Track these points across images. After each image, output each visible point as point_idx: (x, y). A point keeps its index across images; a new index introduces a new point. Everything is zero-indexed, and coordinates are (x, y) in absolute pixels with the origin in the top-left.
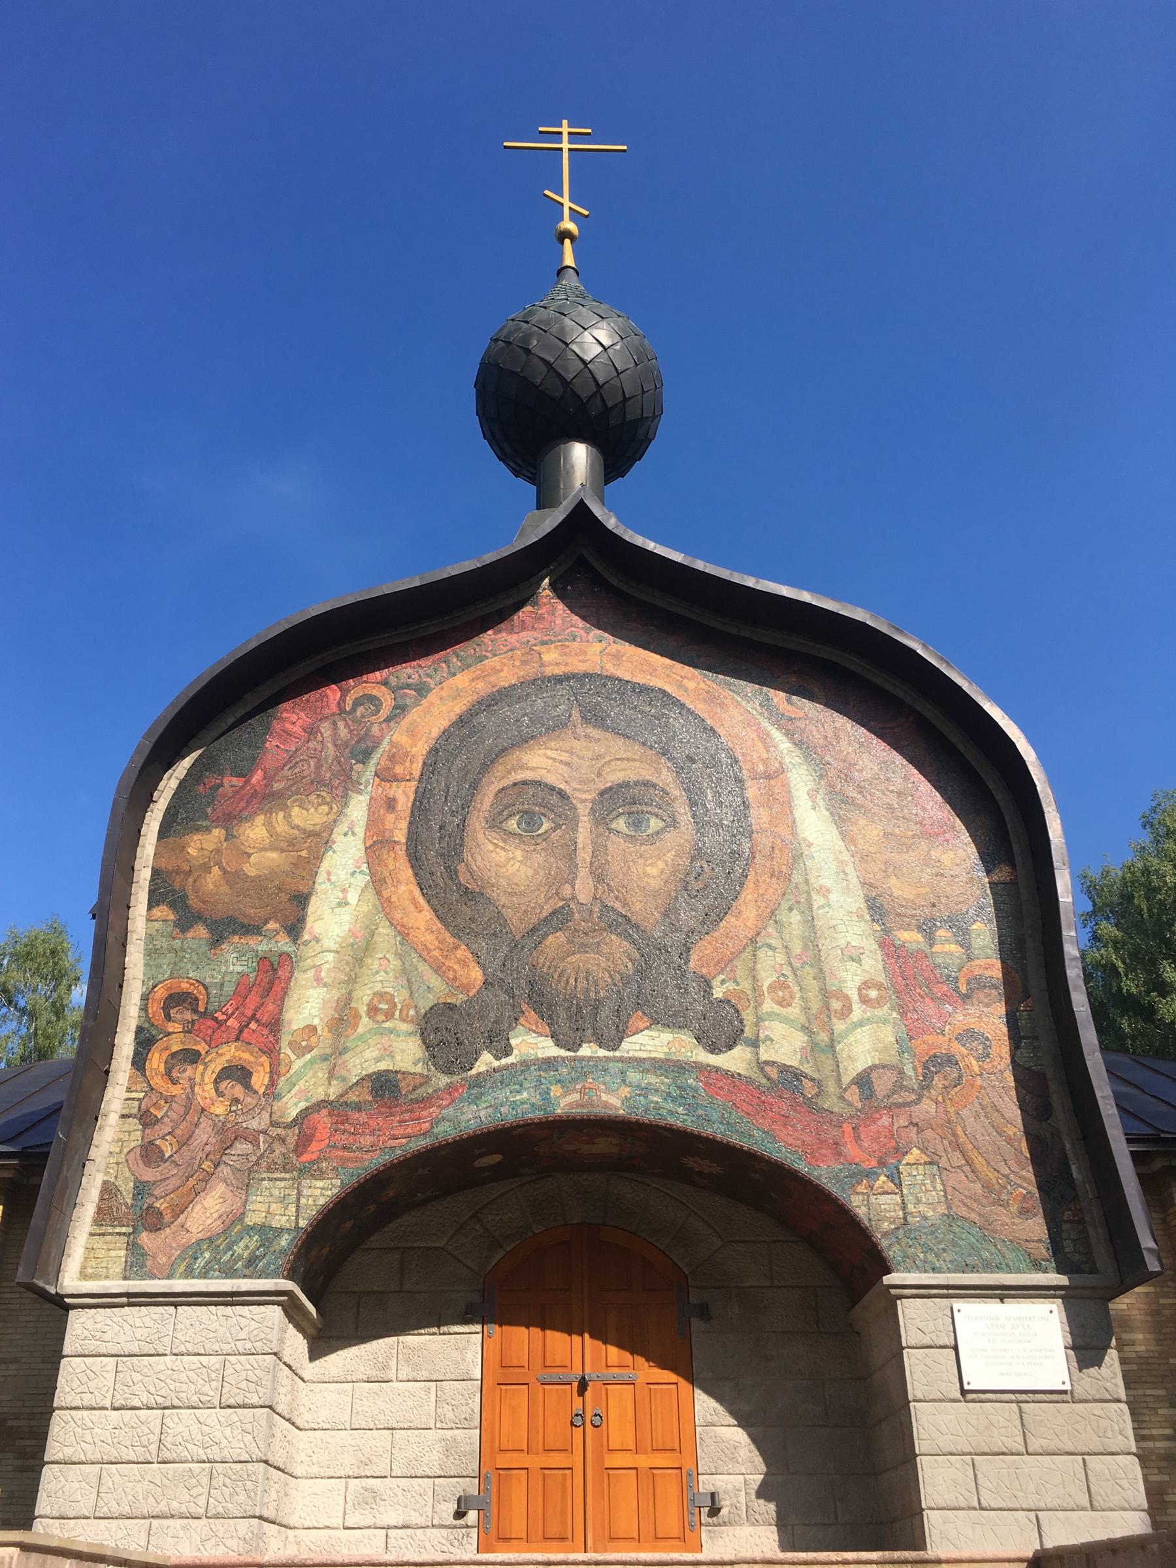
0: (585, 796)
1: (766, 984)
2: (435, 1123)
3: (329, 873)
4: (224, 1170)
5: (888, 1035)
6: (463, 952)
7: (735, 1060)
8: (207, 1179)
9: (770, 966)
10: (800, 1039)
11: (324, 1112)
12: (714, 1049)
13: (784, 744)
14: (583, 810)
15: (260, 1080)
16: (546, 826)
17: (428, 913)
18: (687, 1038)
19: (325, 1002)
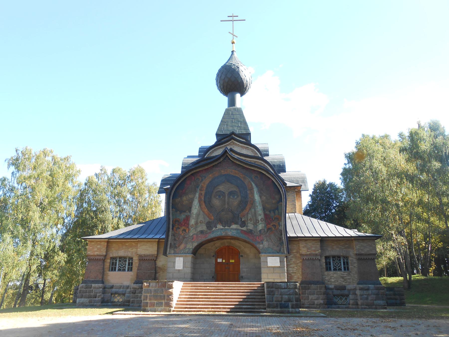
0: (227, 193)
3: (194, 204)
4: (184, 242)
5: (263, 225)
6: (211, 215)
7: (244, 229)
8: (182, 243)
9: (250, 216)
12: (242, 227)
13: (254, 185)
14: (226, 195)
15: (187, 231)
18: (239, 226)
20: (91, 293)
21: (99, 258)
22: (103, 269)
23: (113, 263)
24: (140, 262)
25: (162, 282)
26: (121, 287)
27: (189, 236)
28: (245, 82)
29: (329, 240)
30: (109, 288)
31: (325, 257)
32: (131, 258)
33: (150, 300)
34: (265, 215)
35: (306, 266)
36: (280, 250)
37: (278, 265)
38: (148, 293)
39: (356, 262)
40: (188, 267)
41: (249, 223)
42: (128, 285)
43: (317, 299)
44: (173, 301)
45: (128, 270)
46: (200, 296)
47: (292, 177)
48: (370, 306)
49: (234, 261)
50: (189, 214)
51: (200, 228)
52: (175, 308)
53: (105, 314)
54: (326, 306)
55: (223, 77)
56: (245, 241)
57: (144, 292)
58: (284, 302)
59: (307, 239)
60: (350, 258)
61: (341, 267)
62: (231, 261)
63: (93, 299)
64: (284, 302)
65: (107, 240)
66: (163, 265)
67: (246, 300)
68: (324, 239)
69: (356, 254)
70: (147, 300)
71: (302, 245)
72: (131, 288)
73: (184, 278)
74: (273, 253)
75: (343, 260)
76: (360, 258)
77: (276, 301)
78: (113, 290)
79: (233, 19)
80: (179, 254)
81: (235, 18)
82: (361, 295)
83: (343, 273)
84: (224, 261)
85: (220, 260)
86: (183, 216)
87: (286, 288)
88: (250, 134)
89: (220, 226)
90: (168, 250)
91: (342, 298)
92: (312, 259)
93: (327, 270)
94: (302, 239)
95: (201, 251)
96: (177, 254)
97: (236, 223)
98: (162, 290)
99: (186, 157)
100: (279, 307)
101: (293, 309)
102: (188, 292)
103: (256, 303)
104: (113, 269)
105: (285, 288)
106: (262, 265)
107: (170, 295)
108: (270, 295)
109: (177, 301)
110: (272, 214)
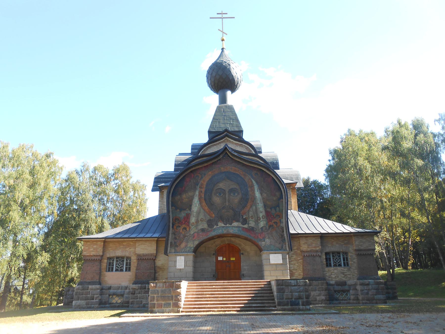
1: (250, 216)
2: (209, 235)
4: (185, 240)
5: (265, 222)
6: (212, 212)
7: (246, 226)
8: (183, 241)
9: (251, 213)
10: (254, 223)
11: (196, 234)
12: (243, 225)
13: (254, 182)
15: (188, 229)
16: (222, 195)
17: (207, 207)
18: (240, 223)
19: (195, 219)
20: (88, 295)
21: (95, 258)
22: (100, 269)
23: (110, 263)
24: (138, 262)
25: (169, 282)
26: (119, 288)
27: (190, 235)
28: (236, 79)
29: (328, 236)
30: (106, 290)
31: (325, 253)
32: (128, 258)
33: (157, 300)
34: (267, 212)
35: (307, 263)
36: (282, 247)
37: (281, 262)
38: (155, 294)
39: (356, 257)
40: (190, 266)
41: (251, 220)
42: (126, 285)
43: (318, 296)
44: (181, 301)
45: (126, 270)
46: (207, 296)
47: (286, 174)
48: (371, 301)
49: (234, 259)
50: (189, 212)
51: (201, 226)
52: (184, 308)
53: (109, 317)
55: (214, 74)
56: (246, 239)
57: (151, 292)
58: (295, 299)
59: (308, 235)
61: (341, 263)
62: (231, 259)
63: (90, 301)
64: (295, 299)
65: (104, 240)
66: (162, 264)
67: (255, 298)
68: (324, 235)
70: (154, 301)
71: (302, 241)
72: (130, 288)
73: (186, 277)
74: (275, 250)
75: (343, 256)
77: (286, 299)
78: (111, 291)
79: (222, 16)
80: (180, 252)
81: (224, 16)
82: (362, 290)
83: (343, 269)
84: (225, 259)
85: (220, 258)
86: (183, 215)
87: (296, 286)
88: (243, 131)
89: (221, 224)
90: (169, 249)
92: (312, 255)
93: (327, 266)
94: (303, 235)
95: (202, 249)
96: (178, 253)
97: (238, 221)
98: (170, 290)
99: (178, 154)
100: (290, 304)
101: (303, 307)
102: (194, 291)
103: (265, 302)
104: (110, 269)
105: (295, 286)
106: (264, 262)
107: (178, 295)
108: (281, 292)
109: (185, 301)
110: (273, 211)
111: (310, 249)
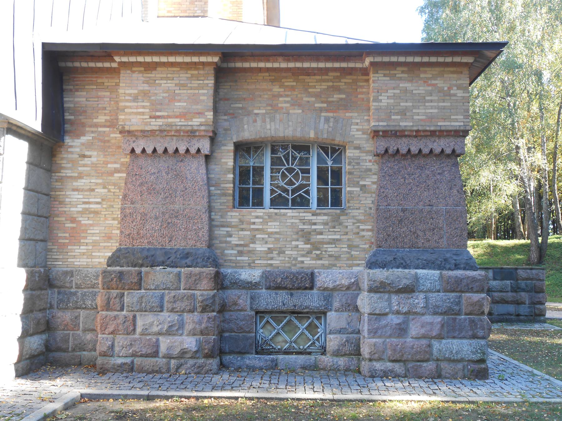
29: (260, 70)
31: (234, 143)
35: (142, 184)
39: (375, 168)
43: (169, 332)
54: (214, 363)
60: (350, 153)
61: (307, 192)
69: (376, 134)
75: (320, 160)
76: (390, 151)
82: (377, 316)
91: (296, 321)
92: (171, 150)
111: (160, 122)
